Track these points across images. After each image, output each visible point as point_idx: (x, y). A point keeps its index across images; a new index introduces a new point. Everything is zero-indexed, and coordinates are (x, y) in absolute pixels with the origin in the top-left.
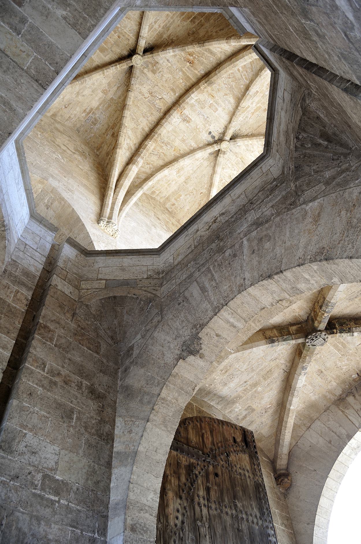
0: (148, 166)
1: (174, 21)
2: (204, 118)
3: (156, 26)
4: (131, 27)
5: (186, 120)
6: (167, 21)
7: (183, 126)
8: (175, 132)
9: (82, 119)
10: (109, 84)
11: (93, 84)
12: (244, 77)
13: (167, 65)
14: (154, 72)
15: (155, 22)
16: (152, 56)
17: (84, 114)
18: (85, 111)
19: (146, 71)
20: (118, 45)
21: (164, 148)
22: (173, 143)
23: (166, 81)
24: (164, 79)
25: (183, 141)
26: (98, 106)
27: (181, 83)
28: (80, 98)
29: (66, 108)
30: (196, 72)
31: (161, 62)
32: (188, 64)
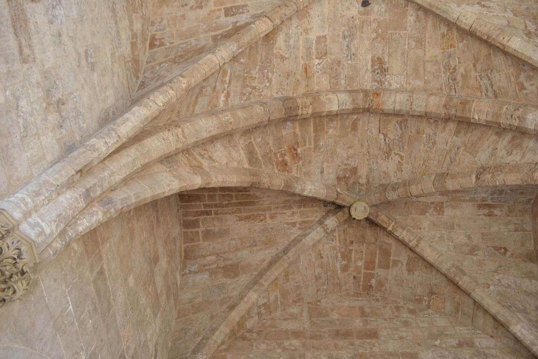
0: (526, 84)
1: (271, 204)
2: (352, 40)
3: (297, 218)
4: (327, 243)
5: (380, 67)
6: (279, 211)
7: (396, 65)
8: (416, 69)
9: (505, 208)
10: (423, 212)
11: (441, 238)
12: (227, 79)
13: (329, 167)
14: (354, 171)
15: (294, 224)
16: (336, 199)
17: (497, 212)
18: (490, 215)
19: (363, 181)
20: (363, 237)
21: (462, 70)
22: (439, 58)
23: (350, 147)
24: (351, 151)
25: (420, 42)
26: (468, 201)
27: (335, 128)
28: (476, 239)
29: (505, 249)
30: (298, 131)
31: (333, 176)
32: (299, 150)
